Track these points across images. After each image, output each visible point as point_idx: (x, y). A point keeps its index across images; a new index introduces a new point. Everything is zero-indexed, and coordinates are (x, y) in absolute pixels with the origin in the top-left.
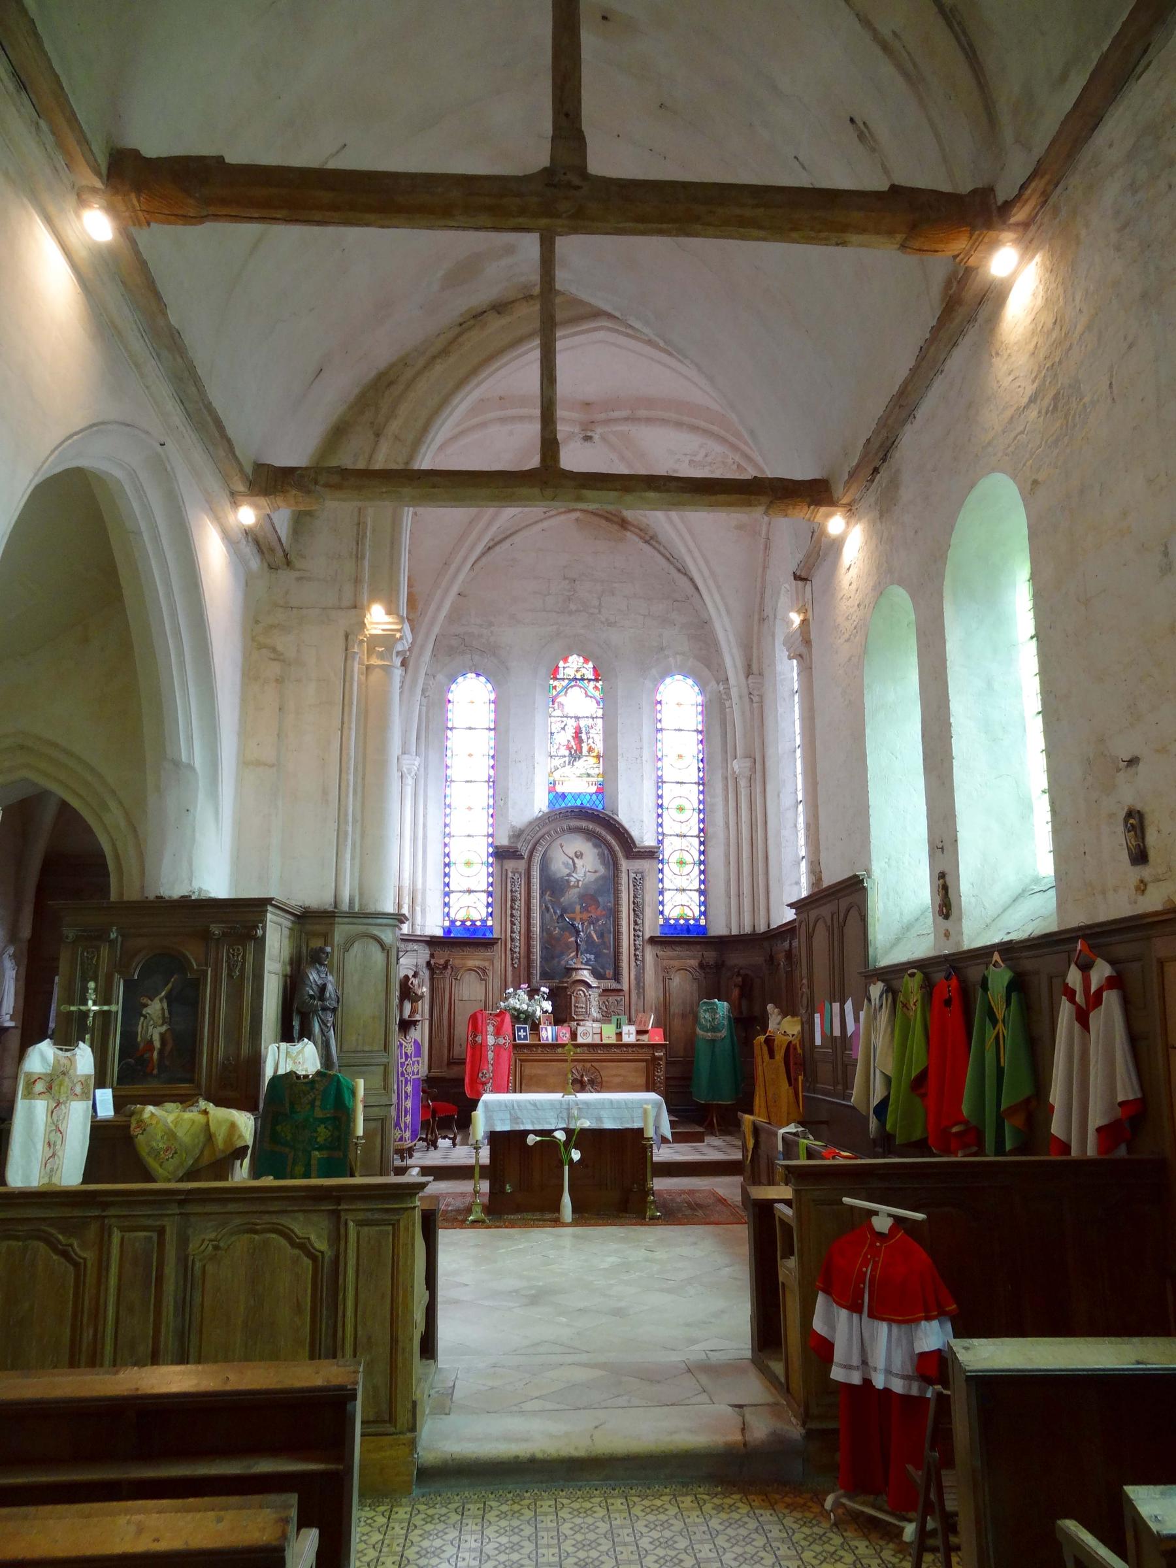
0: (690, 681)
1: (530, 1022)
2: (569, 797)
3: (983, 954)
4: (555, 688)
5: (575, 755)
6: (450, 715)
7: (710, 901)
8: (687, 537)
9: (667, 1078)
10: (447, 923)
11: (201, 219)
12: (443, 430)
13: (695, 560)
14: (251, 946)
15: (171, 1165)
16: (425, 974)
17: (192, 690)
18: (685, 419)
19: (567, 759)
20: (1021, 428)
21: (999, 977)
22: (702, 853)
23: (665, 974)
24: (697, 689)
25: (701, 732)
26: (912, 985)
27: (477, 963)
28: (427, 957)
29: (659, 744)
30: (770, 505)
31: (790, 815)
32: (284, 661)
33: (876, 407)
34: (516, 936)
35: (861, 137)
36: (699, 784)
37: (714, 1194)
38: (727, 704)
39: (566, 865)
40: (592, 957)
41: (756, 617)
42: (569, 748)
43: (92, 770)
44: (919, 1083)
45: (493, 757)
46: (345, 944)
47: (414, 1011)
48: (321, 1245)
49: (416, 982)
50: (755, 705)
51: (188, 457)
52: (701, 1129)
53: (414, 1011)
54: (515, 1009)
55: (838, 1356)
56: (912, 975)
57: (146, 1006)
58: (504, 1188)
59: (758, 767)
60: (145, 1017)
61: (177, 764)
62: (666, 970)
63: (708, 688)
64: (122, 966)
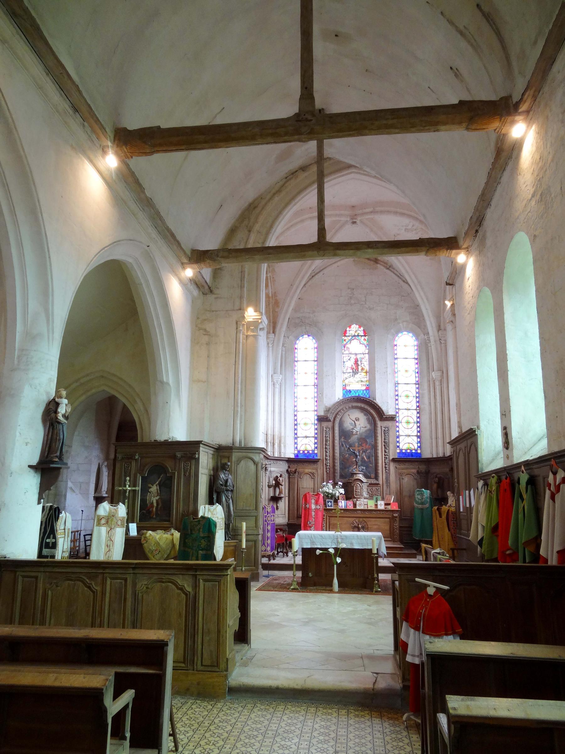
0: (411, 335)
1: (333, 498)
2: (353, 392)
3: (518, 466)
5: (355, 371)
6: (296, 355)
7: (423, 441)
9: (400, 527)
10: (296, 452)
11: (152, 153)
12: (279, 228)
13: (410, 276)
14: (193, 462)
16: (286, 476)
17: (167, 350)
18: (398, 210)
20: (529, 210)
21: (524, 478)
23: (400, 476)
24: (414, 338)
25: (417, 359)
26: (493, 481)
27: (310, 470)
28: (287, 468)
30: (427, 252)
33: (473, 201)
35: (456, 75)
36: (416, 384)
38: (429, 345)
42: (352, 369)
43: (130, 386)
44: (495, 529)
45: (317, 374)
46: (238, 461)
48: (189, 589)
49: (281, 479)
50: (443, 345)
51: (160, 250)
52: (415, 552)
54: (326, 492)
55: (409, 650)
56: (493, 477)
57: (150, 488)
58: (308, 574)
61: (162, 382)
62: (401, 474)
63: (420, 338)
64: (140, 470)
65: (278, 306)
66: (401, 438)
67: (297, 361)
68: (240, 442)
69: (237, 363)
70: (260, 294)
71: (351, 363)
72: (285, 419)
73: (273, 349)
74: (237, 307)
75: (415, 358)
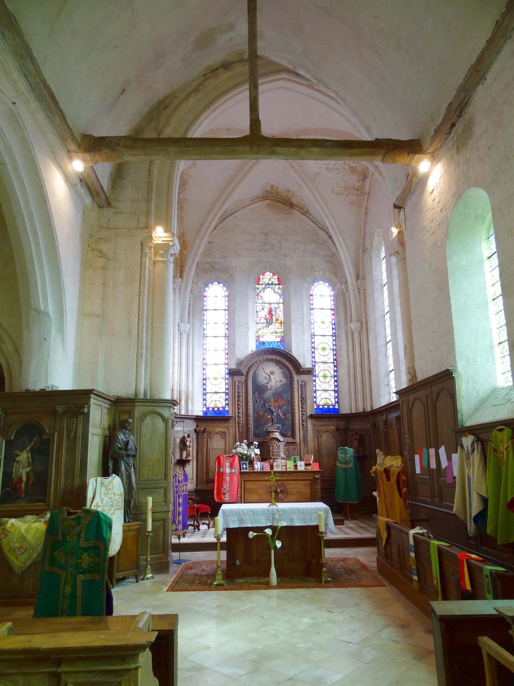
1: (248, 460)
2: (267, 344)
5: (269, 322)
6: (205, 303)
8: (325, 209)
9: (322, 489)
10: (205, 409)
14: (81, 418)
15: (22, 558)
16: (194, 436)
17: (46, 267)
19: (265, 324)
23: (318, 434)
24: (330, 288)
25: (333, 310)
27: (220, 429)
28: (195, 427)
29: (312, 316)
31: (382, 349)
32: (107, 258)
33: (457, 79)
34: (241, 415)
36: (333, 336)
37: (358, 561)
38: (347, 295)
39: (266, 378)
40: (280, 425)
41: (361, 249)
42: (266, 319)
45: (227, 324)
46: (141, 417)
47: (188, 455)
49: (188, 439)
50: (361, 294)
52: (342, 518)
53: (188, 455)
54: (240, 453)
57: (18, 455)
58: (235, 562)
59: (364, 326)
60: (18, 462)
61: (38, 311)
62: (319, 432)
63: (337, 287)
66: (318, 393)
67: (206, 310)
68: (145, 393)
69: (141, 293)
71: (264, 313)
72: (193, 372)
73: (179, 296)
74: (141, 225)
75: (331, 309)
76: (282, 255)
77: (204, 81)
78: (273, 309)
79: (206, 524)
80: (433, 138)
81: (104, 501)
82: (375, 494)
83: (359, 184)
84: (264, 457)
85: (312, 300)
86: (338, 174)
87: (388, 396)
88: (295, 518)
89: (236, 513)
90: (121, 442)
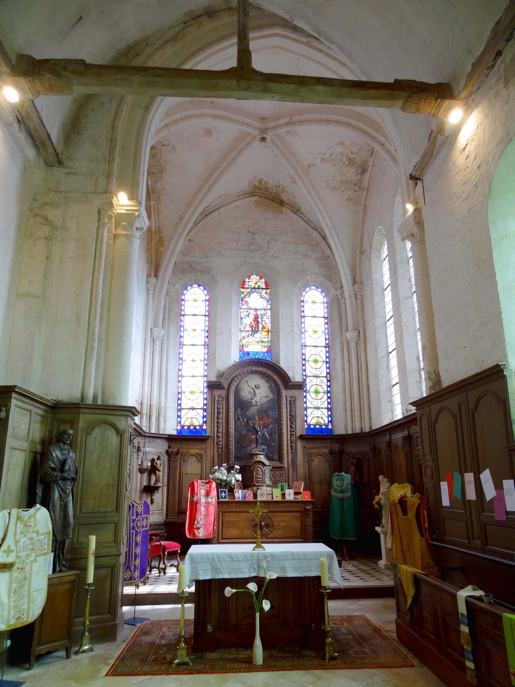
1: (228, 487)
2: (251, 354)
4: (243, 293)
5: (255, 330)
7: (334, 414)
8: (319, 204)
10: (179, 428)
16: (165, 458)
22: (329, 386)
23: (309, 457)
27: (197, 451)
29: (303, 325)
31: (384, 361)
36: (326, 347)
37: (367, 621)
38: (342, 301)
39: (250, 393)
40: (266, 447)
41: (358, 251)
42: (251, 326)
45: (207, 331)
46: (88, 428)
47: (157, 481)
49: (158, 462)
50: (359, 301)
53: (157, 481)
54: (219, 479)
58: (206, 628)
59: (362, 335)
62: (310, 455)
63: (330, 294)
65: (162, 245)
66: (309, 411)
67: (184, 315)
68: (95, 398)
69: (96, 272)
70: (140, 166)
71: (249, 321)
73: (153, 297)
75: (324, 317)
76: (270, 257)
77: (184, 29)
78: (259, 316)
79: (175, 566)
80: (470, 76)
81: (21, 544)
82: (378, 529)
83: (358, 179)
84: (246, 484)
85: (303, 306)
86: (334, 166)
87: (390, 415)
88: (288, 566)
89: (208, 558)
90: (55, 460)
